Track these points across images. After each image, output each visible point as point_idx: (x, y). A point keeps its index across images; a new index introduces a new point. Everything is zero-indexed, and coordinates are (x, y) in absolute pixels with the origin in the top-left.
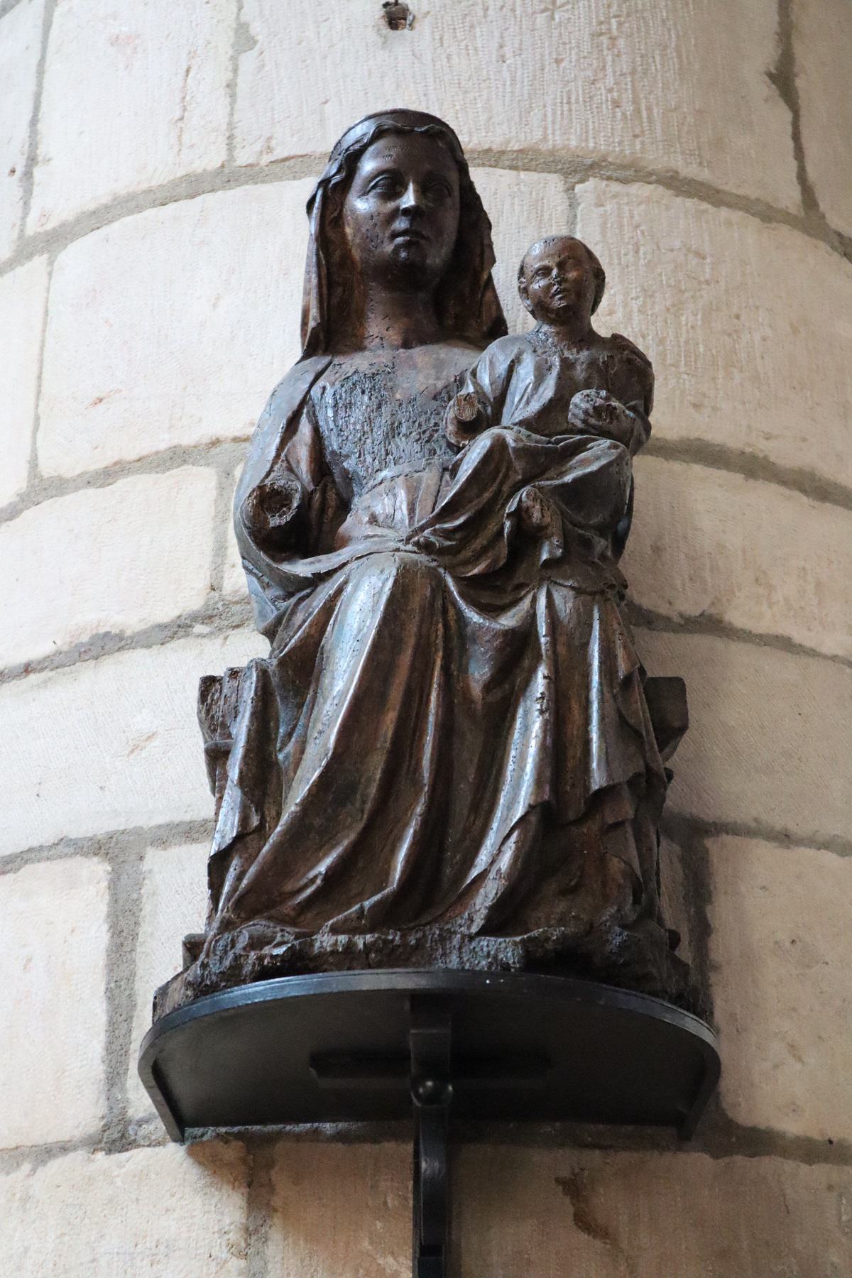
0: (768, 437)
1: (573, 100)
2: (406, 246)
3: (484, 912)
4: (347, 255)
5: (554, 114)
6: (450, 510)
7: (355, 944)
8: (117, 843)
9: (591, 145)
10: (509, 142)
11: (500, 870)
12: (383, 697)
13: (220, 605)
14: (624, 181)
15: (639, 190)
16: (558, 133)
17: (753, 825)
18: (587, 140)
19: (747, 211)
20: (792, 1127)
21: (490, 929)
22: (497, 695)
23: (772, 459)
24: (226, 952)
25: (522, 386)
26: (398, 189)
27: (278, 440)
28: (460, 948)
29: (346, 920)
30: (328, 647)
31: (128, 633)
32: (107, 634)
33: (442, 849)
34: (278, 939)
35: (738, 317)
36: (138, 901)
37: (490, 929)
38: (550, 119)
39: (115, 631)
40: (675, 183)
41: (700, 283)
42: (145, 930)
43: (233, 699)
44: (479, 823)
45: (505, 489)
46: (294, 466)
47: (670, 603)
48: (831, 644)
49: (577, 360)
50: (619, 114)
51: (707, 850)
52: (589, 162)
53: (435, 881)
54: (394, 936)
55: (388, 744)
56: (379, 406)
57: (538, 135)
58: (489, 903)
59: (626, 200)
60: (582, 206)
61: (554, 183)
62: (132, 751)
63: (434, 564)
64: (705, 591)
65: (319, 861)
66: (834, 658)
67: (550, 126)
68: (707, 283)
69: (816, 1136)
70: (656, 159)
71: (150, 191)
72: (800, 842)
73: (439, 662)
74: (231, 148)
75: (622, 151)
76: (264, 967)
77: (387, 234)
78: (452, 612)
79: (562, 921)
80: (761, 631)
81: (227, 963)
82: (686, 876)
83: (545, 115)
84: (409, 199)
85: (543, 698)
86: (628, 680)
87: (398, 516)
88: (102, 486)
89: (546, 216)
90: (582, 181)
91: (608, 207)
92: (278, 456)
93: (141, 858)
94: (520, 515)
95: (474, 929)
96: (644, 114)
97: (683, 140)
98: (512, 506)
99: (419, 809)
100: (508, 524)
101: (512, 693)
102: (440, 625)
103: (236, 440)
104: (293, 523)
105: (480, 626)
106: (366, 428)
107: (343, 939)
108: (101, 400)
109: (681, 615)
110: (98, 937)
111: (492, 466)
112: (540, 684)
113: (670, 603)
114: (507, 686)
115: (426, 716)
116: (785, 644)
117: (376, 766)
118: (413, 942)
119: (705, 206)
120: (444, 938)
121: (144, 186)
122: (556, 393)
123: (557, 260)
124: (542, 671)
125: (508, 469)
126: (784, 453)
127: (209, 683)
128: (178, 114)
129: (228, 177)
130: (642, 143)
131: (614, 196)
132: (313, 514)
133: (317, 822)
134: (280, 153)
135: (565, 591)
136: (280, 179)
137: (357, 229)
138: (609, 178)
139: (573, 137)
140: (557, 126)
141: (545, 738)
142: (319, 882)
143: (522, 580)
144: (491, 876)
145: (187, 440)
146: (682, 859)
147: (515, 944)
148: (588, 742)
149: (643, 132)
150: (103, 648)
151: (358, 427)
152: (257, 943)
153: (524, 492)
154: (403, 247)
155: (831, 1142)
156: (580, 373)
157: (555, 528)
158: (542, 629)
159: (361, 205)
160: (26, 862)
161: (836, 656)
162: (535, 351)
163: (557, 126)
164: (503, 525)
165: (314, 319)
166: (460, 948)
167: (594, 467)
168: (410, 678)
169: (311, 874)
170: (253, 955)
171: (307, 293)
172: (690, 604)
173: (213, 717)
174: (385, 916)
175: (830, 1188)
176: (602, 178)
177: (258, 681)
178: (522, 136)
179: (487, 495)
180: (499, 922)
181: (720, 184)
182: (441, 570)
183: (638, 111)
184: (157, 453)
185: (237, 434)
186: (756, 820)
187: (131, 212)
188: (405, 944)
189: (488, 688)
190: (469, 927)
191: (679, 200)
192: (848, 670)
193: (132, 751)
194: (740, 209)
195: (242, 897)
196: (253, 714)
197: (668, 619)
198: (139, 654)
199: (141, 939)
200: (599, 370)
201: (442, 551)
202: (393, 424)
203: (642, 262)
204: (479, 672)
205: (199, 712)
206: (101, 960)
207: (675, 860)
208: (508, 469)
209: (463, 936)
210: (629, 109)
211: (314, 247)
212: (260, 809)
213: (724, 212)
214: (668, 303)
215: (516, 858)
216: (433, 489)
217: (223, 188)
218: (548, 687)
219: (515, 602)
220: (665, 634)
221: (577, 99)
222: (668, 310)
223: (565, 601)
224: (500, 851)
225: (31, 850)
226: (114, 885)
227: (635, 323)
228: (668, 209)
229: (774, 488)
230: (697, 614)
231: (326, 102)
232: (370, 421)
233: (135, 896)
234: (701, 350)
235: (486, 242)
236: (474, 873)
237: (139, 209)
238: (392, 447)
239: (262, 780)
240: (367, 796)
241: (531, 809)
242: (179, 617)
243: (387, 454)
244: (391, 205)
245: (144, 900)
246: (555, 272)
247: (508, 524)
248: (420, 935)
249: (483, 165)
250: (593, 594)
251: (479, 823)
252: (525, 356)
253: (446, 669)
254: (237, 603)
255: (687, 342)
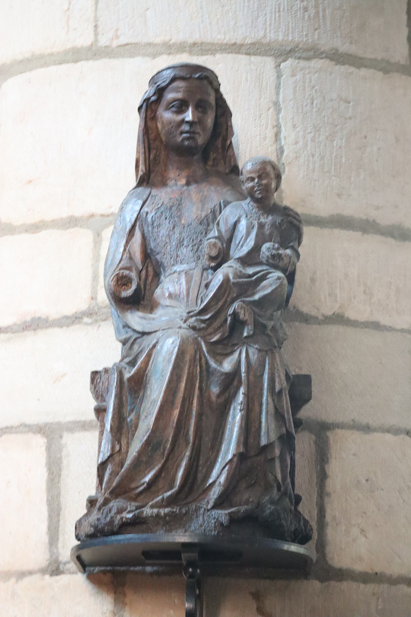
0: (377, 208)
1: (281, 9)
2: (188, 139)
3: (213, 500)
4: (158, 135)
5: (271, 19)
6: (203, 312)
7: (160, 513)
8: (49, 428)
9: (290, 38)
10: (245, 39)
11: (220, 483)
12: (173, 403)
13: (96, 308)
14: (308, 59)
15: (317, 64)
16: (272, 32)
17: (352, 423)
18: (288, 35)
19: (375, 68)
20: (359, 567)
21: (216, 506)
22: (222, 400)
23: (378, 221)
24: (107, 514)
25: (239, 237)
26: (184, 108)
27: (125, 241)
28: (204, 514)
29: (156, 503)
30: (149, 375)
31: (51, 319)
32: (39, 318)
33: (197, 466)
34: (129, 509)
35: (365, 137)
36: (60, 458)
37: (216, 506)
38: (268, 23)
39: (43, 317)
40: (337, 57)
41: (346, 119)
42: (64, 473)
43: (106, 384)
44: (214, 455)
45: (229, 299)
46: (133, 256)
47: (318, 309)
48: (401, 322)
49: (266, 223)
50: (306, 17)
51: (328, 437)
52: (289, 48)
53: (194, 484)
54: (176, 510)
55: (175, 425)
56: (174, 228)
57: (262, 34)
58: (215, 497)
59: (307, 71)
60: (284, 77)
61: (269, 62)
62: (55, 382)
63: (196, 335)
64: (336, 301)
65: (145, 476)
66: (402, 330)
67: (268, 27)
68: (350, 118)
69: (370, 571)
70: (327, 42)
71: (51, 55)
72: (375, 430)
73: (197, 385)
74: (96, 34)
75: (307, 40)
76: (123, 522)
77: (178, 132)
78: (203, 359)
79: (247, 503)
80: (363, 320)
81: (108, 519)
82: (317, 451)
83: (266, 21)
84: (189, 116)
85: (241, 403)
86: (280, 392)
87: (182, 296)
88: (33, 233)
89: (264, 84)
90: (285, 61)
91: (298, 77)
92: (125, 250)
93: (61, 437)
94: (235, 315)
95: (209, 507)
96: (321, 14)
97: (342, 28)
98: (231, 311)
99: (188, 453)
100: (229, 319)
101: (229, 398)
102: (198, 368)
103: (102, 215)
104: (133, 293)
105: (216, 370)
106: (167, 240)
107: (155, 510)
108: (31, 182)
109: (323, 315)
110: (40, 475)
111: (223, 290)
112: (241, 397)
113: (318, 309)
114: (227, 394)
115: (192, 414)
116: (376, 326)
117: (170, 433)
118: (184, 512)
119: (352, 69)
120: (197, 509)
121: (49, 51)
122: (255, 244)
123: (257, 174)
124: (242, 390)
125: (230, 291)
126: (385, 218)
127: (95, 374)
128: (66, 7)
129: (94, 52)
130: (319, 34)
131: (301, 70)
132: (142, 287)
133: (144, 459)
134: (123, 40)
135: (254, 350)
136: (123, 57)
137: (163, 127)
138: (299, 58)
139: (280, 34)
140: (272, 27)
141: (241, 423)
142: (145, 485)
143: (235, 342)
144: (217, 483)
145: (78, 213)
146: (315, 442)
147: (226, 514)
148: (260, 423)
149: (319, 26)
150: (38, 325)
151: (164, 239)
152: (120, 511)
153: (236, 305)
154: (186, 132)
155: (376, 573)
156: (267, 230)
157: (251, 321)
158: (243, 369)
159: (167, 116)
160: (5, 433)
161: (403, 329)
162: (247, 216)
163: (272, 27)
164: (226, 320)
165: (142, 170)
166: (204, 514)
167: (269, 291)
168: (184, 394)
169: (143, 481)
170: (118, 517)
171: (138, 152)
172: (328, 308)
173: (97, 391)
174: (171, 501)
175: (374, 594)
176: (295, 59)
177: (117, 377)
178: (253, 35)
179: (220, 304)
180: (219, 504)
181: (360, 53)
182: (199, 339)
183: (317, 13)
184: (62, 219)
185: (104, 212)
186: (353, 420)
187: (42, 66)
188: (180, 512)
189: (218, 396)
190: (207, 506)
191: (338, 67)
192: (408, 336)
193: (55, 382)
194: (371, 68)
195: (114, 489)
196: (116, 395)
197: (316, 318)
198: (56, 331)
199: (62, 477)
200: (276, 227)
201: (200, 330)
202: (180, 239)
203: (315, 110)
204: (215, 390)
205: (91, 389)
206: (43, 485)
207: (312, 443)
208: (230, 291)
209: (205, 510)
210: (312, 11)
211: (142, 134)
212: (119, 442)
213: (363, 72)
214: (327, 134)
215: (227, 479)
216: (198, 282)
217: (93, 59)
218: (244, 398)
219: (232, 353)
220: (314, 326)
221: (284, 9)
222: (327, 138)
223: (254, 356)
224: (221, 473)
225: (7, 428)
226: (49, 449)
227: (309, 148)
228: (331, 74)
229: (378, 238)
230: (332, 314)
231: (148, 9)
232: (169, 236)
233: (59, 456)
234: (344, 161)
235: (229, 124)
236: (211, 481)
237: (46, 65)
238: (179, 253)
239: (121, 429)
240: (166, 447)
241: (234, 455)
242: (76, 313)
243: (177, 256)
244: (180, 118)
245: (63, 457)
246: (256, 180)
247: (229, 319)
248: (187, 508)
249: (232, 52)
250: (266, 351)
251: (214, 455)
252: (242, 219)
253: (201, 389)
254: (105, 307)
255: (336, 157)
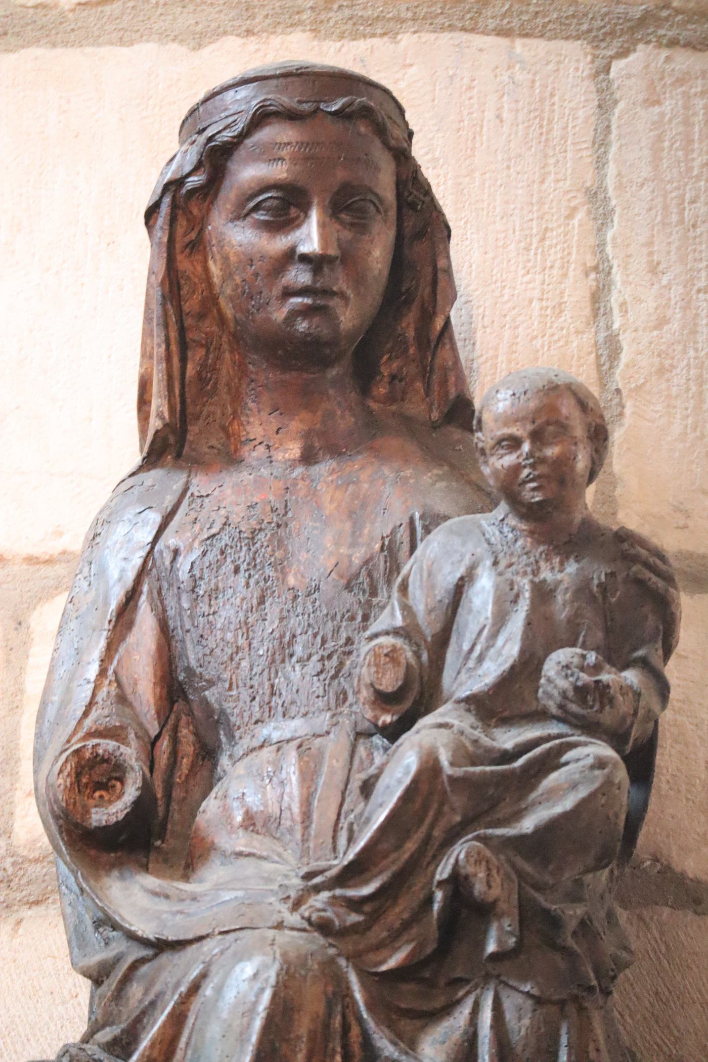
4: (211, 300)
6: (354, 872)
26: (293, 211)
27: (102, 643)
45: (436, 833)
46: (128, 690)
56: (262, 601)
60: (621, 105)
63: (332, 951)
77: (276, 291)
78: (355, 1031)
84: (310, 237)
87: (286, 823)
89: (556, 133)
90: (623, 53)
91: (668, 106)
92: (103, 672)
94: (457, 883)
98: (443, 871)
100: (439, 895)
103: (31, 560)
106: (241, 641)
111: (419, 801)
122: (522, 652)
123: (530, 427)
131: (680, 81)
135: (519, 999)
136: (96, 42)
137: (228, 275)
138: (673, 43)
143: (458, 974)
153: (460, 851)
156: (562, 608)
157: (509, 904)
159: (237, 237)
162: (495, 563)
164: (429, 900)
165: (160, 416)
167: (567, 804)
171: (146, 355)
176: (660, 45)
179: (411, 846)
182: (342, 962)
185: (35, 551)
201: (343, 933)
202: (282, 637)
211: (157, 294)
216: (340, 776)
219: (447, 1009)
223: (521, 1022)
232: (246, 627)
235: (441, 263)
238: (279, 681)
243: (273, 694)
244: (281, 243)
247: (439, 895)
249: (451, 28)
250: (562, 1003)
252: (479, 570)
254: (36, 861)
